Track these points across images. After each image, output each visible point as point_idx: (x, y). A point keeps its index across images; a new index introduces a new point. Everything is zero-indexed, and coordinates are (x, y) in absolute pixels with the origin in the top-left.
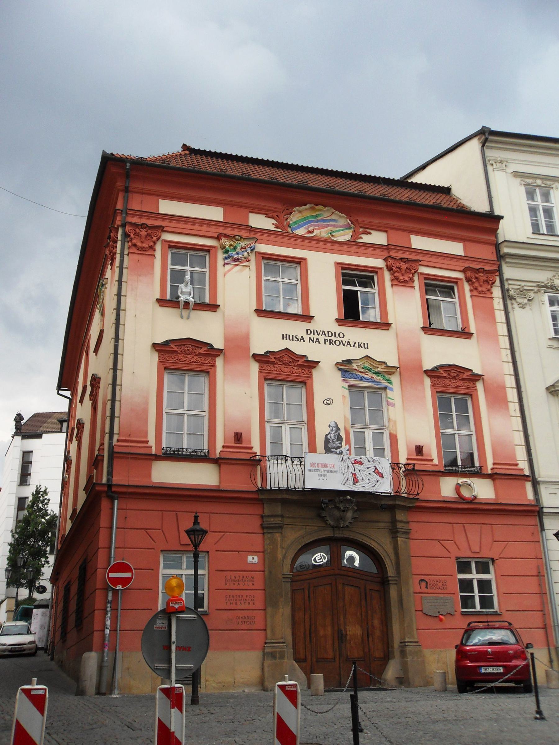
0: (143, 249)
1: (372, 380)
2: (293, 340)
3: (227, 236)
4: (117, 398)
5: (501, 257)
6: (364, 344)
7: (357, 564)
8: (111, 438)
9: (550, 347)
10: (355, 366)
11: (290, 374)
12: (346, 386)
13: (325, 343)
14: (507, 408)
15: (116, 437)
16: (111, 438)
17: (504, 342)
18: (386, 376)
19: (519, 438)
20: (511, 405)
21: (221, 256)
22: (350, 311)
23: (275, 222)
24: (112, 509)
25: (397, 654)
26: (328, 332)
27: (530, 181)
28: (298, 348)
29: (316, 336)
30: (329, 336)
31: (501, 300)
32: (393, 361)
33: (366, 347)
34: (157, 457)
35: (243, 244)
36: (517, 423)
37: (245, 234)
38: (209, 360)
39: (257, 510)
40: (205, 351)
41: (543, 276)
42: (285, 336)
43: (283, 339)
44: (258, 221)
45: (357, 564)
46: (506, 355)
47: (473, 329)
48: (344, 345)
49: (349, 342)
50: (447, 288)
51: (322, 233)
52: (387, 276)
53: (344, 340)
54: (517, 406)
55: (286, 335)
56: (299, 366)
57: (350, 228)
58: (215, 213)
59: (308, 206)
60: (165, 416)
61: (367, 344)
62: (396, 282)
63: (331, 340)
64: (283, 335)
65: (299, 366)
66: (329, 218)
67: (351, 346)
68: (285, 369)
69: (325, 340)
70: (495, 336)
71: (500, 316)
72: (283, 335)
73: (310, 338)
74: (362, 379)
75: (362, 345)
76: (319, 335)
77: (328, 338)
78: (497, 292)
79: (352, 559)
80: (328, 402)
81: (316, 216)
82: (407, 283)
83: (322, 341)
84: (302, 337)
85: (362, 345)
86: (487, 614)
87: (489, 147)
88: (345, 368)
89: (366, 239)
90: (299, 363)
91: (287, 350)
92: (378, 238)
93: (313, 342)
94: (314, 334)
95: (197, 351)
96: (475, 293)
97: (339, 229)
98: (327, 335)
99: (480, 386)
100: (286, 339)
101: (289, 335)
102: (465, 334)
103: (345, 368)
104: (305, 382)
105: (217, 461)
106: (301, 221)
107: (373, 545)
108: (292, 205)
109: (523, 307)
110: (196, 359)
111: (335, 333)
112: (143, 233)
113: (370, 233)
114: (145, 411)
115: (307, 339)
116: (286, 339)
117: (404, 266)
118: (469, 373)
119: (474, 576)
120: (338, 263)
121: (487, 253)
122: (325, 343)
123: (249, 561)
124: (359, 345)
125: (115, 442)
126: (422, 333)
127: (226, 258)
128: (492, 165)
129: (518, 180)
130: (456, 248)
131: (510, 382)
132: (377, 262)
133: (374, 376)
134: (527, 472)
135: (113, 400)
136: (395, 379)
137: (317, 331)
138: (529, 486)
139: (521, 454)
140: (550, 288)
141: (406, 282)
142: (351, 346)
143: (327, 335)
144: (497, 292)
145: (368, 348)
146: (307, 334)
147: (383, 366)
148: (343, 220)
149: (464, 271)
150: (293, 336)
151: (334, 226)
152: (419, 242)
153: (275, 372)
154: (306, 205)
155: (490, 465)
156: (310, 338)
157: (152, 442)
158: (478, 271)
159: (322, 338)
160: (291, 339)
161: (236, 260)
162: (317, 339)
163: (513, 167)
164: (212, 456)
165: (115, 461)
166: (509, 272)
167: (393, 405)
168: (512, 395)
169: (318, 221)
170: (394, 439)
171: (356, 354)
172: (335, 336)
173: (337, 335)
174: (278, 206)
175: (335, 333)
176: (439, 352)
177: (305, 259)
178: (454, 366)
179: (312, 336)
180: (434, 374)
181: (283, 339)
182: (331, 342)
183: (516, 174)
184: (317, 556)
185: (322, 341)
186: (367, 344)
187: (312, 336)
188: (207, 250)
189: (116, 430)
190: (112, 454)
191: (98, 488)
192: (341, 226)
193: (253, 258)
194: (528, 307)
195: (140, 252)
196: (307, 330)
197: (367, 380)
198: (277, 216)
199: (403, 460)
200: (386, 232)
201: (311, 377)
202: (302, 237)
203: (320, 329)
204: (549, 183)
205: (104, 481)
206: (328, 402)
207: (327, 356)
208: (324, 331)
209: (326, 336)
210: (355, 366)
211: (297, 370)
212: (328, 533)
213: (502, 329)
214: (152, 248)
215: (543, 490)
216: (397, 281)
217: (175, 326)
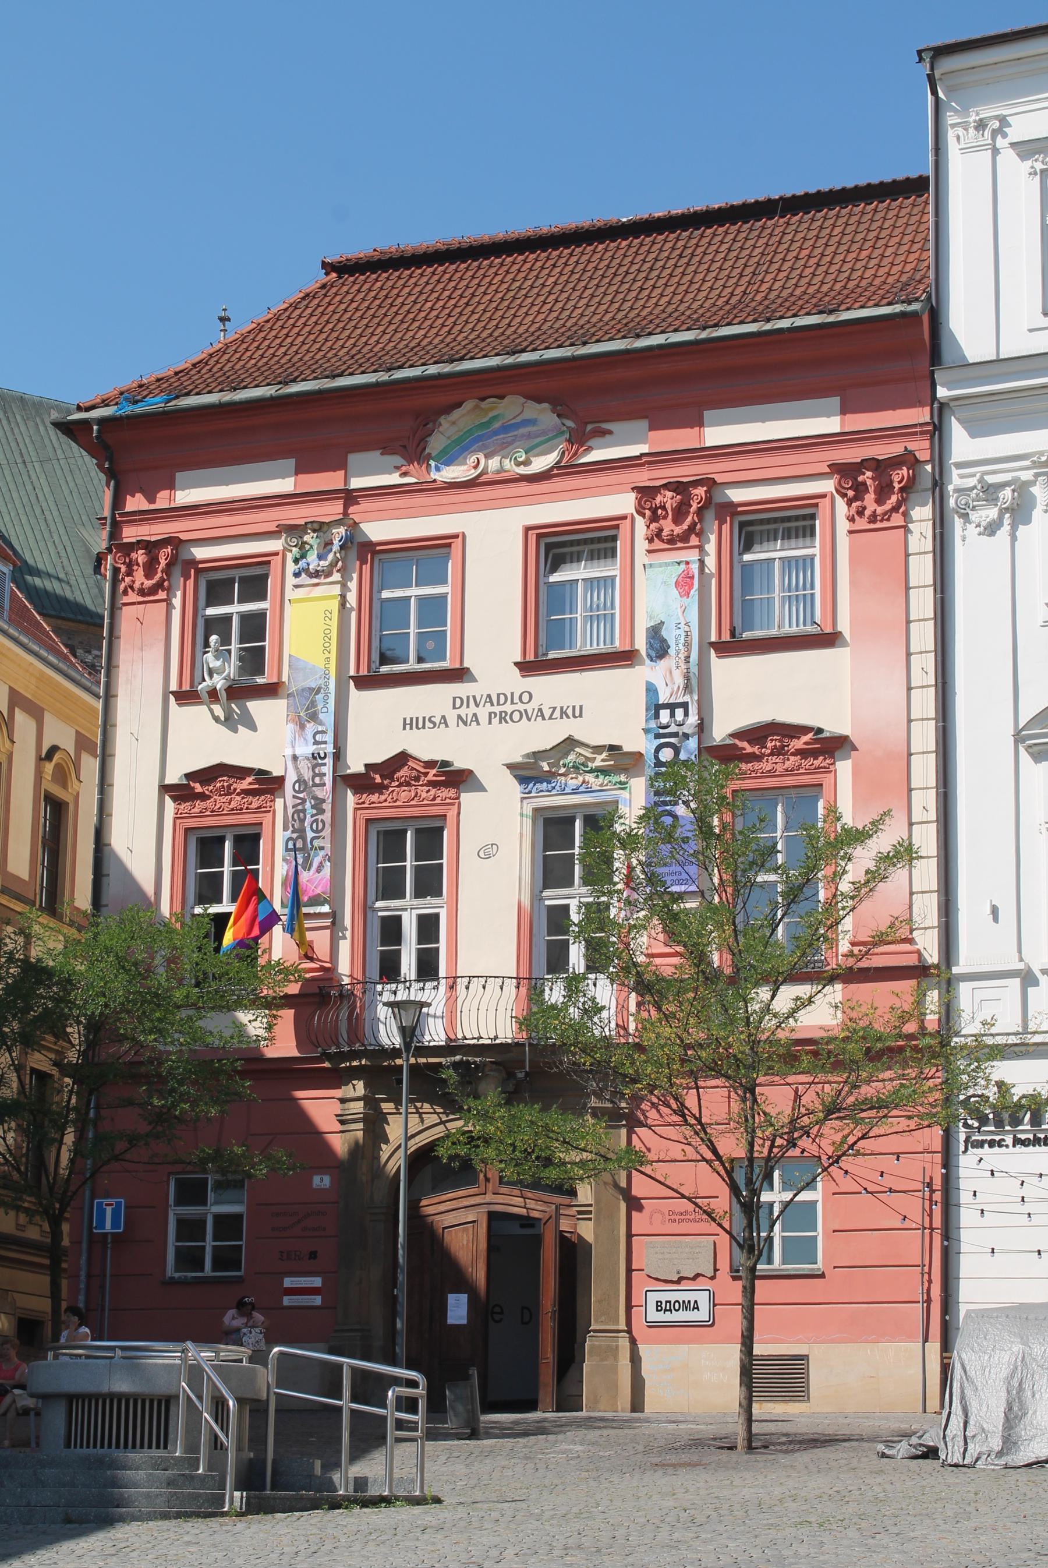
2: (424, 727)
6: (574, 707)
11: (412, 803)
13: (490, 723)
21: (291, 567)
26: (498, 695)
28: (425, 747)
29: (473, 708)
30: (498, 704)
33: (577, 714)
40: (250, 784)
42: (408, 721)
43: (404, 728)
46: (924, 668)
48: (529, 719)
49: (540, 710)
50: (796, 521)
53: (529, 707)
55: (411, 719)
56: (431, 783)
59: (468, 405)
61: (581, 707)
62: (658, 544)
64: (405, 719)
65: (431, 783)
66: (519, 419)
67: (544, 719)
68: (404, 795)
69: (490, 714)
71: (922, 570)
72: (405, 719)
73: (459, 717)
75: (570, 712)
76: (477, 705)
77: (497, 709)
80: (487, 852)
81: (489, 423)
83: (483, 718)
84: (443, 717)
85: (570, 712)
88: (528, 773)
90: (430, 777)
93: (465, 723)
94: (468, 707)
96: (862, 523)
97: (539, 440)
98: (495, 703)
100: (411, 728)
101: (417, 719)
111: (512, 694)
113: (610, 432)
115: (452, 720)
116: (411, 728)
118: (810, 735)
120: (527, 529)
122: (490, 723)
123: (314, 1186)
124: (563, 713)
127: (297, 575)
128: (958, 138)
131: (925, 736)
134: (932, 957)
137: (474, 697)
140: (1047, 468)
142: (544, 719)
143: (495, 703)
145: (581, 716)
146: (454, 707)
147: (604, 755)
148: (545, 416)
150: (424, 718)
153: (384, 804)
154: (459, 405)
156: (459, 717)
159: (483, 712)
160: (420, 726)
162: (475, 715)
168: (925, 771)
169: (496, 433)
171: (545, 736)
172: (512, 703)
173: (516, 700)
175: (512, 694)
179: (463, 711)
181: (404, 728)
182: (502, 719)
185: (483, 718)
186: (581, 707)
187: (463, 711)
192: (544, 433)
195: (146, 599)
196: (454, 699)
197: (575, 791)
198: (404, 447)
200: (646, 417)
206: (487, 852)
208: (489, 696)
209: (492, 705)
211: (423, 791)
213: (923, 603)
217: (201, 739)
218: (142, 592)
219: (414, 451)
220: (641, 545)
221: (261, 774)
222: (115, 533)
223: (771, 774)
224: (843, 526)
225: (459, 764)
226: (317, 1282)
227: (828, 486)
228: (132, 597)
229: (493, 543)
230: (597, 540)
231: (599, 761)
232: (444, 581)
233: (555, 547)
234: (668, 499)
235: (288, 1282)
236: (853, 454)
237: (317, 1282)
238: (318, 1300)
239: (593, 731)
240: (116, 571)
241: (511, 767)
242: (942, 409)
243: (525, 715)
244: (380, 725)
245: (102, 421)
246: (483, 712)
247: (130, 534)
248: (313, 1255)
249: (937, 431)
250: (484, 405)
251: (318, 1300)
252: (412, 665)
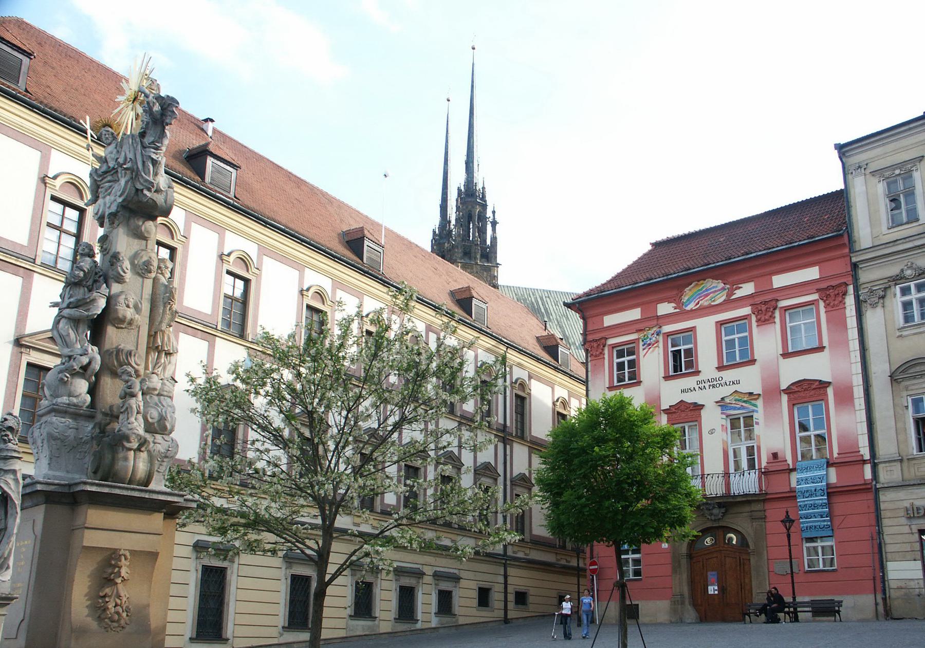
0: (596, 356)
1: (743, 408)
3: (641, 330)
5: (855, 266)
7: (734, 542)
10: (727, 400)
12: (724, 416)
14: (853, 405)
17: (855, 345)
19: (863, 428)
20: (857, 402)
27: (887, 174)
28: (689, 398)
32: (757, 390)
35: (652, 332)
36: (862, 416)
37: (655, 322)
44: (665, 308)
45: (734, 542)
46: (856, 356)
47: (826, 343)
51: (705, 302)
57: (723, 289)
58: (635, 314)
70: (846, 342)
71: (852, 322)
74: (735, 409)
78: (850, 300)
79: (731, 539)
80: (712, 432)
82: (770, 320)
83: (707, 387)
86: (828, 571)
87: (847, 157)
88: (722, 403)
89: (739, 293)
91: (682, 401)
92: (748, 289)
99: (830, 391)
102: (821, 349)
103: (722, 403)
104: (698, 419)
106: (691, 298)
107: (739, 529)
108: (681, 288)
109: (874, 306)
112: (595, 345)
115: (697, 388)
117: (764, 308)
120: (717, 322)
121: (840, 267)
126: (781, 358)
130: (812, 273)
131: (857, 381)
132: (747, 311)
133: (744, 404)
134: (867, 456)
136: (760, 402)
138: (868, 468)
139: (863, 442)
141: (768, 320)
144: (850, 300)
149: (818, 290)
151: (715, 291)
155: (835, 455)
158: (827, 288)
159: (707, 385)
161: (649, 344)
163: (873, 167)
166: (865, 276)
167: (757, 423)
168: (859, 392)
170: (759, 448)
174: (675, 292)
176: (794, 371)
177: (694, 327)
178: (804, 380)
180: (788, 391)
183: (873, 173)
184: (708, 539)
185: (707, 387)
193: (661, 338)
194: (880, 305)
197: (739, 409)
199: (764, 464)
201: (700, 416)
202: (692, 310)
203: (705, 379)
206: (712, 432)
207: (707, 398)
210: (727, 400)
211: (690, 414)
212: (709, 525)
213: (853, 333)
214: (602, 353)
215: (881, 468)
216: (761, 322)
219: (677, 300)
220: (754, 324)
223: (805, 398)
225: (700, 403)
227: (815, 297)
229: (705, 327)
236: (824, 285)
239: (744, 388)
241: (717, 402)
242: (855, 266)
243: (721, 385)
246: (707, 385)
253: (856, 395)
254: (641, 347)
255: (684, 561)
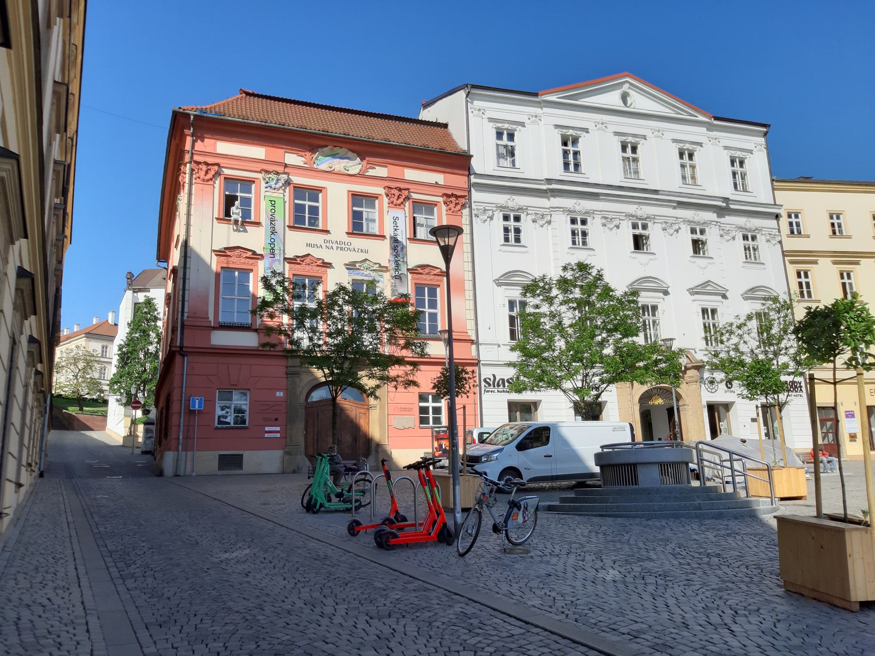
4: (187, 288)
8: (182, 315)
9: (500, 250)
15: (186, 315)
16: (182, 315)
18: (381, 273)
21: (263, 184)
22: (357, 227)
23: (303, 159)
24: (183, 362)
25: (373, 453)
27: (499, 125)
28: (316, 253)
31: (468, 218)
34: (214, 328)
38: (251, 261)
39: (283, 362)
41: (501, 199)
44: (292, 159)
52: (386, 200)
54: (471, 293)
59: (329, 147)
60: (221, 299)
63: (342, 247)
68: (307, 267)
78: (466, 212)
83: (335, 248)
88: (351, 266)
89: (371, 172)
91: (308, 255)
92: (381, 171)
95: (245, 255)
96: (450, 212)
105: (256, 330)
110: (243, 260)
114: (207, 297)
115: (324, 245)
119: (430, 404)
125: (185, 318)
129: (492, 124)
131: (468, 276)
135: (184, 289)
139: (470, 325)
152: (411, 174)
157: (211, 317)
163: (489, 114)
164: (253, 327)
165: (186, 331)
171: (360, 257)
182: (341, 249)
183: (491, 120)
185: (335, 248)
188: (252, 181)
189: (186, 310)
190: (183, 326)
191: (173, 349)
204: (514, 126)
205: (178, 344)
217: (228, 236)
218: (204, 180)
221: (254, 253)
222: (192, 157)
224: (444, 212)
226: (278, 429)
227: (441, 199)
228: (198, 181)
230: (371, 199)
231: (376, 267)
232: (317, 201)
233: (357, 198)
234: (397, 193)
235: (267, 429)
236: (449, 192)
237: (278, 429)
238: (278, 435)
240: (192, 170)
241: (346, 265)
242: (470, 185)
244: (297, 243)
245: (195, 116)
247: (196, 158)
248: (276, 419)
249: (470, 192)
250: (335, 149)
251: (278, 435)
252: (307, 226)
253: (466, 288)
254: (263, 189)
255: (302, 412)
